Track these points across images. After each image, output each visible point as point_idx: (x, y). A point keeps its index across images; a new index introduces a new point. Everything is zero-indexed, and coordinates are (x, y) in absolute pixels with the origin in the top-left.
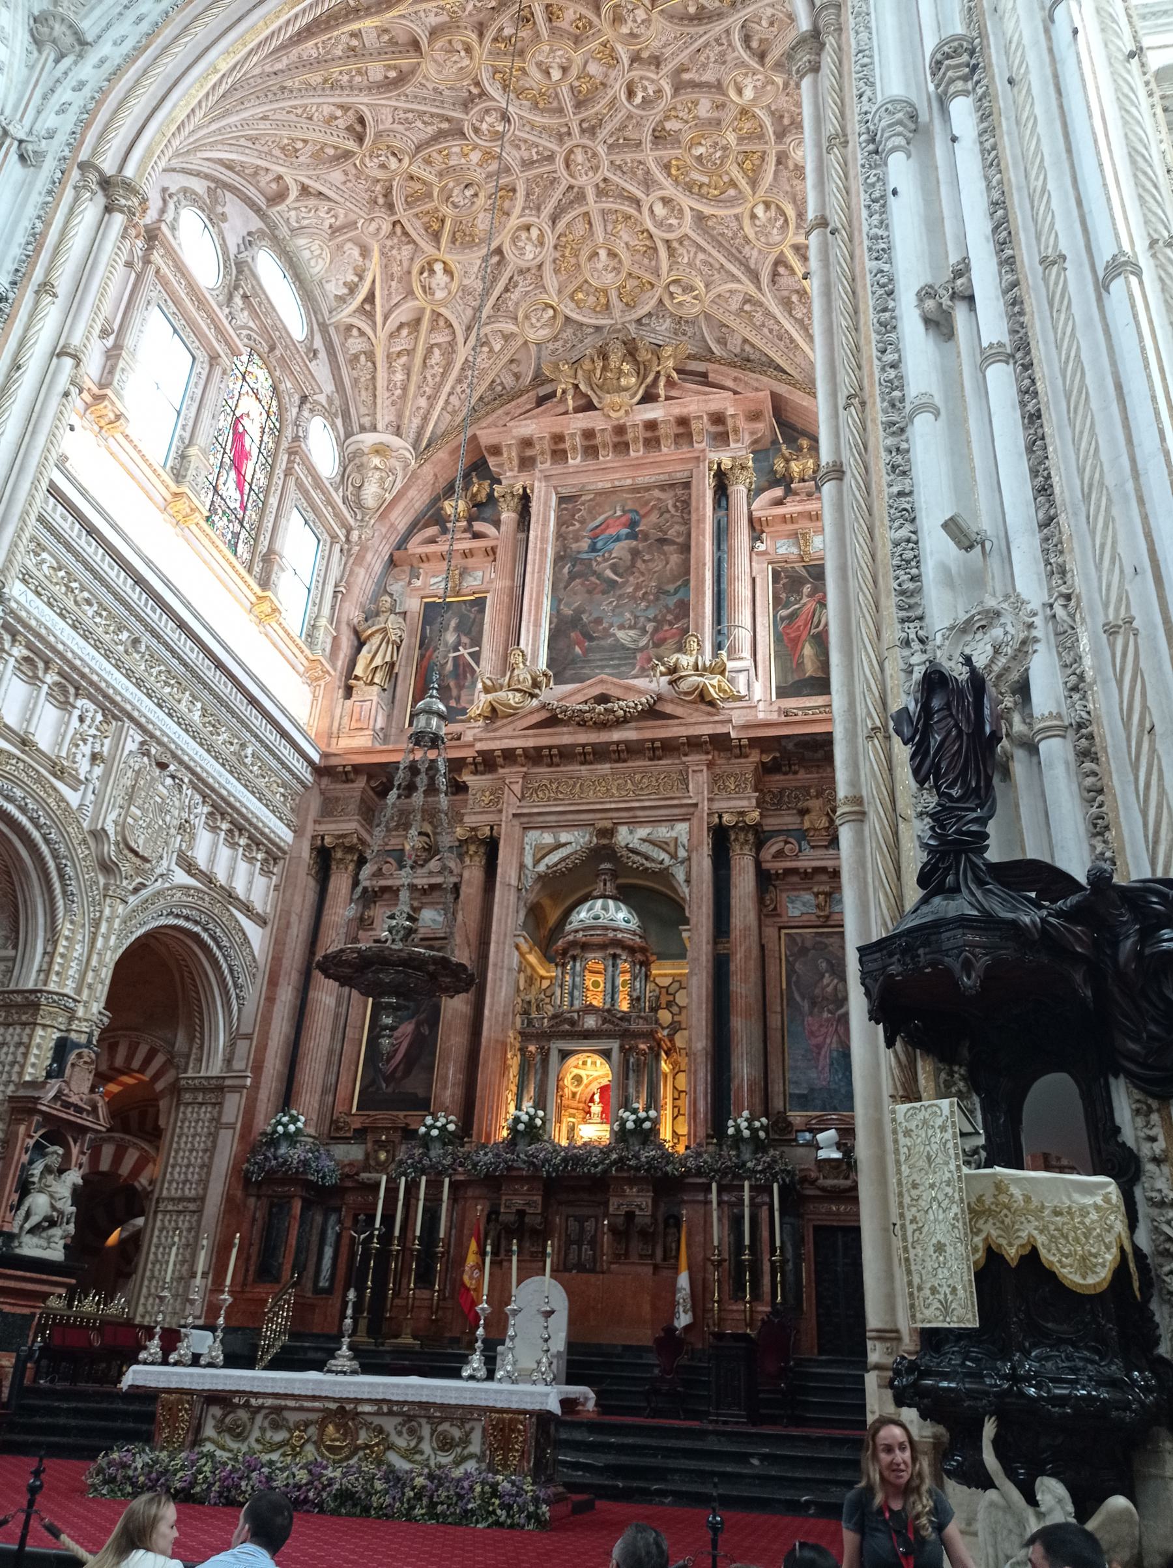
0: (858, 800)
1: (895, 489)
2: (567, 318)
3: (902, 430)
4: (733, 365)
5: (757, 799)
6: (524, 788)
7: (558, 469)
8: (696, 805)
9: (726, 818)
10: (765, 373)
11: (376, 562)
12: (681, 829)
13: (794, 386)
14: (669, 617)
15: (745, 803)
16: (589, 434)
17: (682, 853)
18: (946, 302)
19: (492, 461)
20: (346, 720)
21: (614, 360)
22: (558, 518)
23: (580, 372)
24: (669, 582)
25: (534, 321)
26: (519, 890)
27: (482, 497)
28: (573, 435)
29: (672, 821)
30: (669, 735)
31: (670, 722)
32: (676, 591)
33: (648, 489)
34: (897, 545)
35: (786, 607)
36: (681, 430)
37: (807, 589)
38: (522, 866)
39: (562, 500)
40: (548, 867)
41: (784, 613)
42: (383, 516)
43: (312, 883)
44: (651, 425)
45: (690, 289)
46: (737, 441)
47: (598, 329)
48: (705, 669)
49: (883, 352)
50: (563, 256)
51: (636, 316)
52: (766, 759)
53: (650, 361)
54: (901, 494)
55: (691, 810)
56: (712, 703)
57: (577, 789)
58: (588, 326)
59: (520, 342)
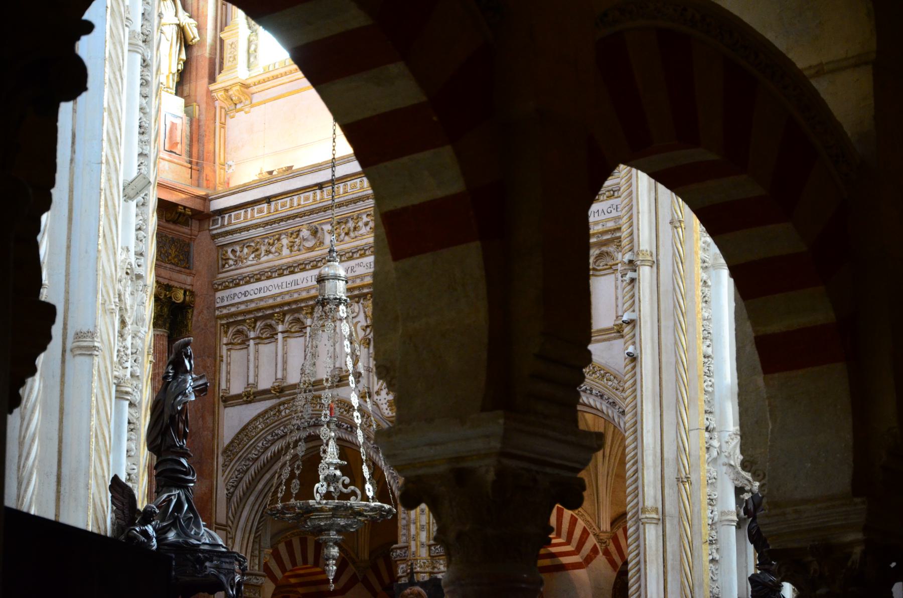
0: (656, 510)
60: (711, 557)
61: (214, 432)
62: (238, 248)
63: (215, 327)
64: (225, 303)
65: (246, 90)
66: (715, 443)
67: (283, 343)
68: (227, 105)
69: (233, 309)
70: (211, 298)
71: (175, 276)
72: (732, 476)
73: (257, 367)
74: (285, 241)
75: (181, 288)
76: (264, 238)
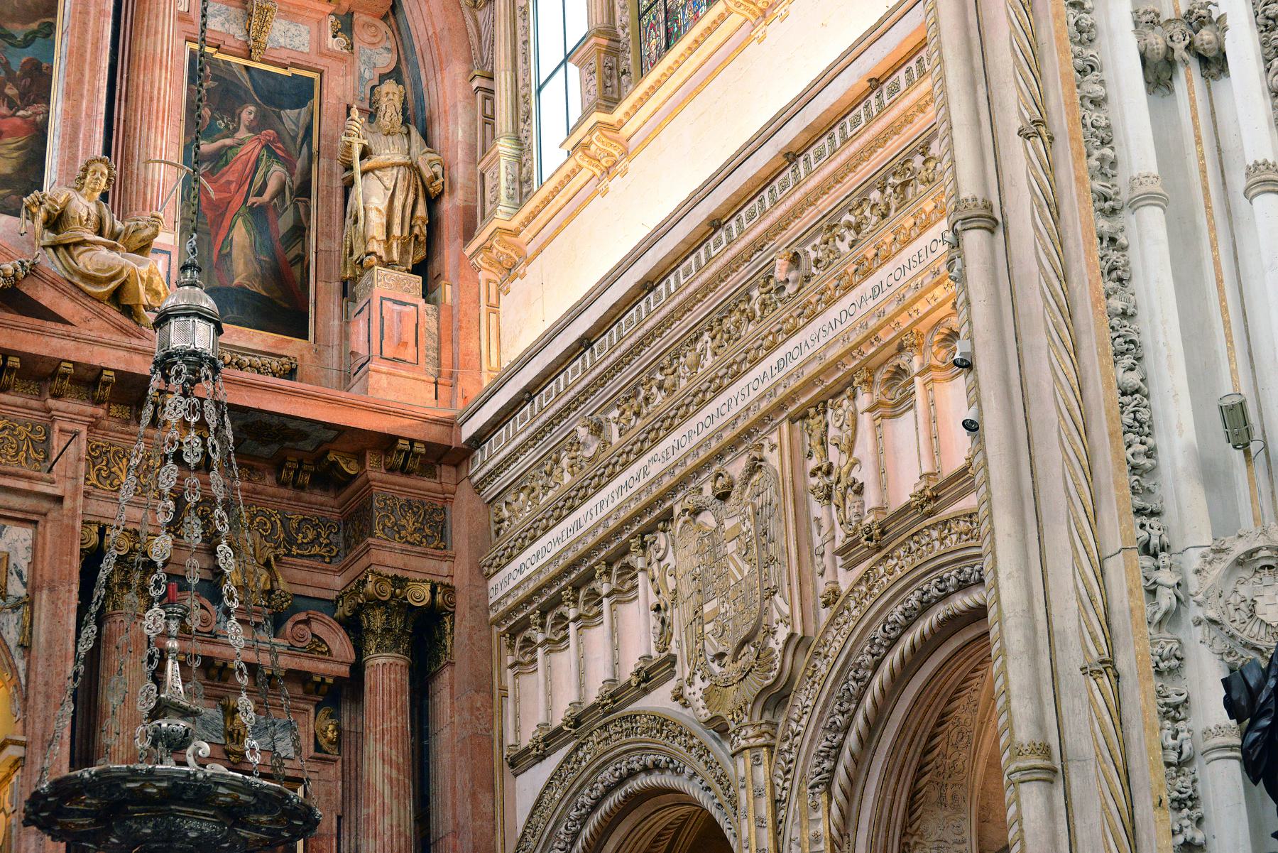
0: (1046, 751)
1: (1117, 304)
3: (1114, 211)
8: (59, 500)
9: (112, 534)
14: (11, 91)
18: (1179, 48)
24: (13, 18)
30: (44, 351)
31: (50, 325)
32: (28, 41)
34: (1124, 394)
35: (210, 133)
37: (248, 114)
41: (206, 147)
48: (115, 236)
49: (1082, 72)
54: (1124, 314)
55: (45, 505)
56: (129, 311)
60: (1180, 839)
61: (493, 820)
62: (510, 498)
63: (490, 640)
64: (500, 594)
65: (514, 239)
66: (1166, 577)
67: (578, 639)
69: (510, 601)
70: (480, 591)
71: (415, 562)
72: (1218, 646)
73: (549, 694)
74: (565, 462)
75: (425, 581)
76: (539, 464)
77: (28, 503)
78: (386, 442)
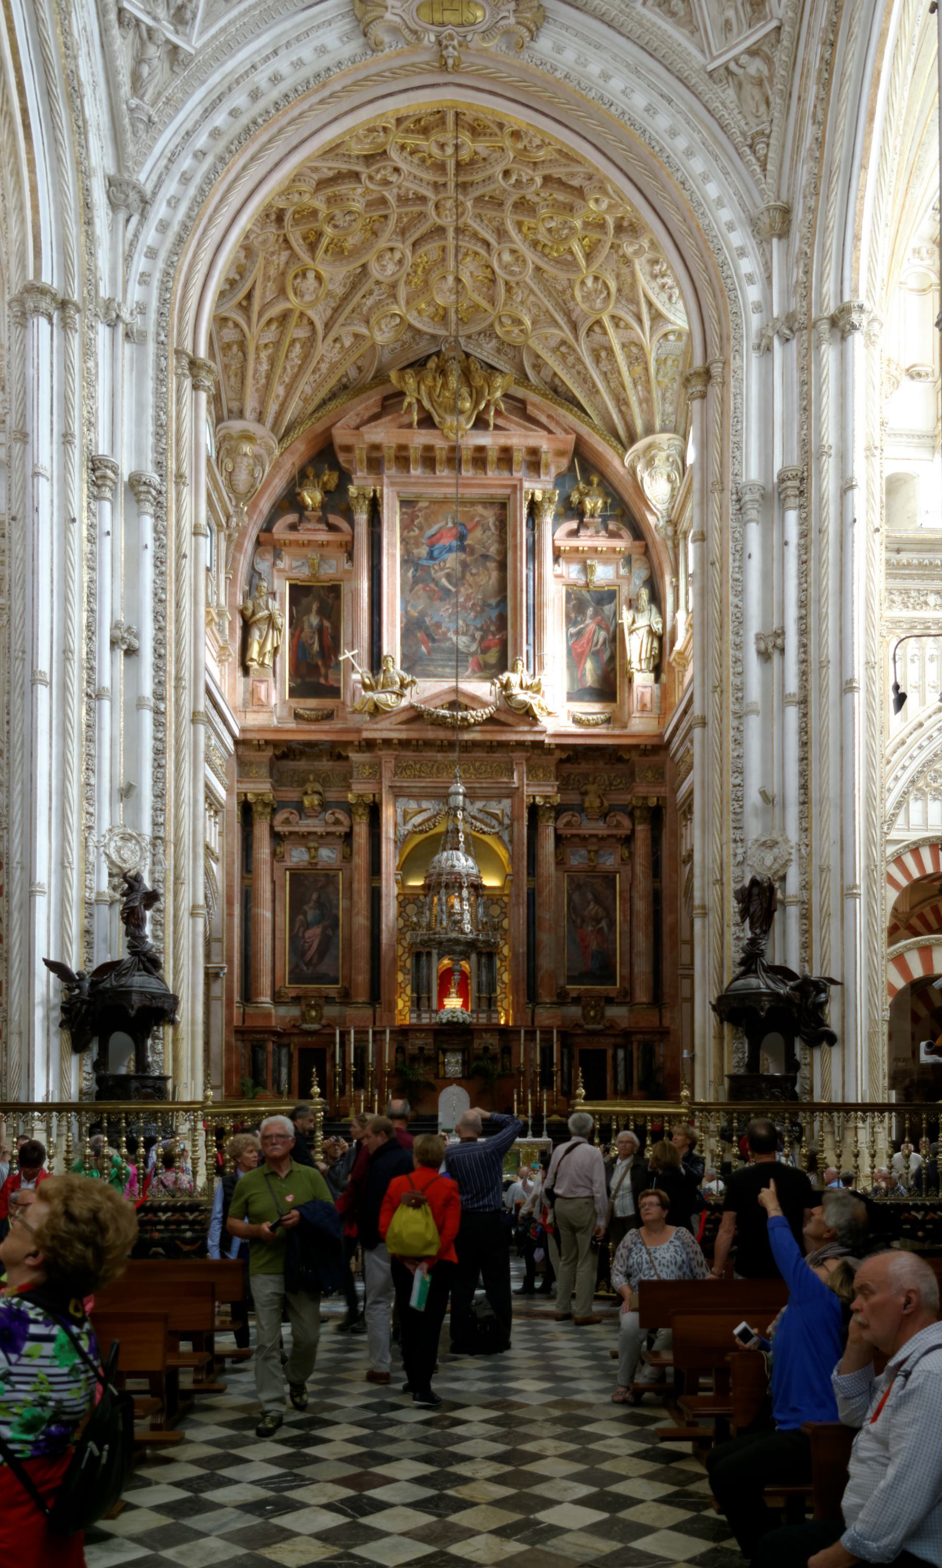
2: (410, 327)
4: (545, 395)
5: (559, 788)
6: (396, 766)
7: (401, 477)
9: (538, 799)
10: (571, 411)
11: (249, 545)
12: (506, 803)
13: (593, 429)
15: (550, 789)
16: (429, 448)
17: (507, 821)
19: (342, 457)
20: (248, 696)
21: (453, 382)
22: (401, 521)
23: (423, 387)
25: (383, 327)
26: (395, 842)
27: (332, 484)
28: (416, 448)
29: (499, 797)
33: (473, 503)
36: (502, 456)
38: (396, 825)
39: (404, 503)
40: (415, 826)
42: (254, 506)
43: (237, 828)
44: (481, 449)
45: (518, 322)
46: (547, 474)
47: (434, 337)
50: (415, 272)
51: (467, 332)
52: (564, 756)
53: (482, 387)
57: (435, 770)
58: (425, 333)
59: (368, 344)
68: (681, 669)
77: (508, 791)
78: (636, 747)
